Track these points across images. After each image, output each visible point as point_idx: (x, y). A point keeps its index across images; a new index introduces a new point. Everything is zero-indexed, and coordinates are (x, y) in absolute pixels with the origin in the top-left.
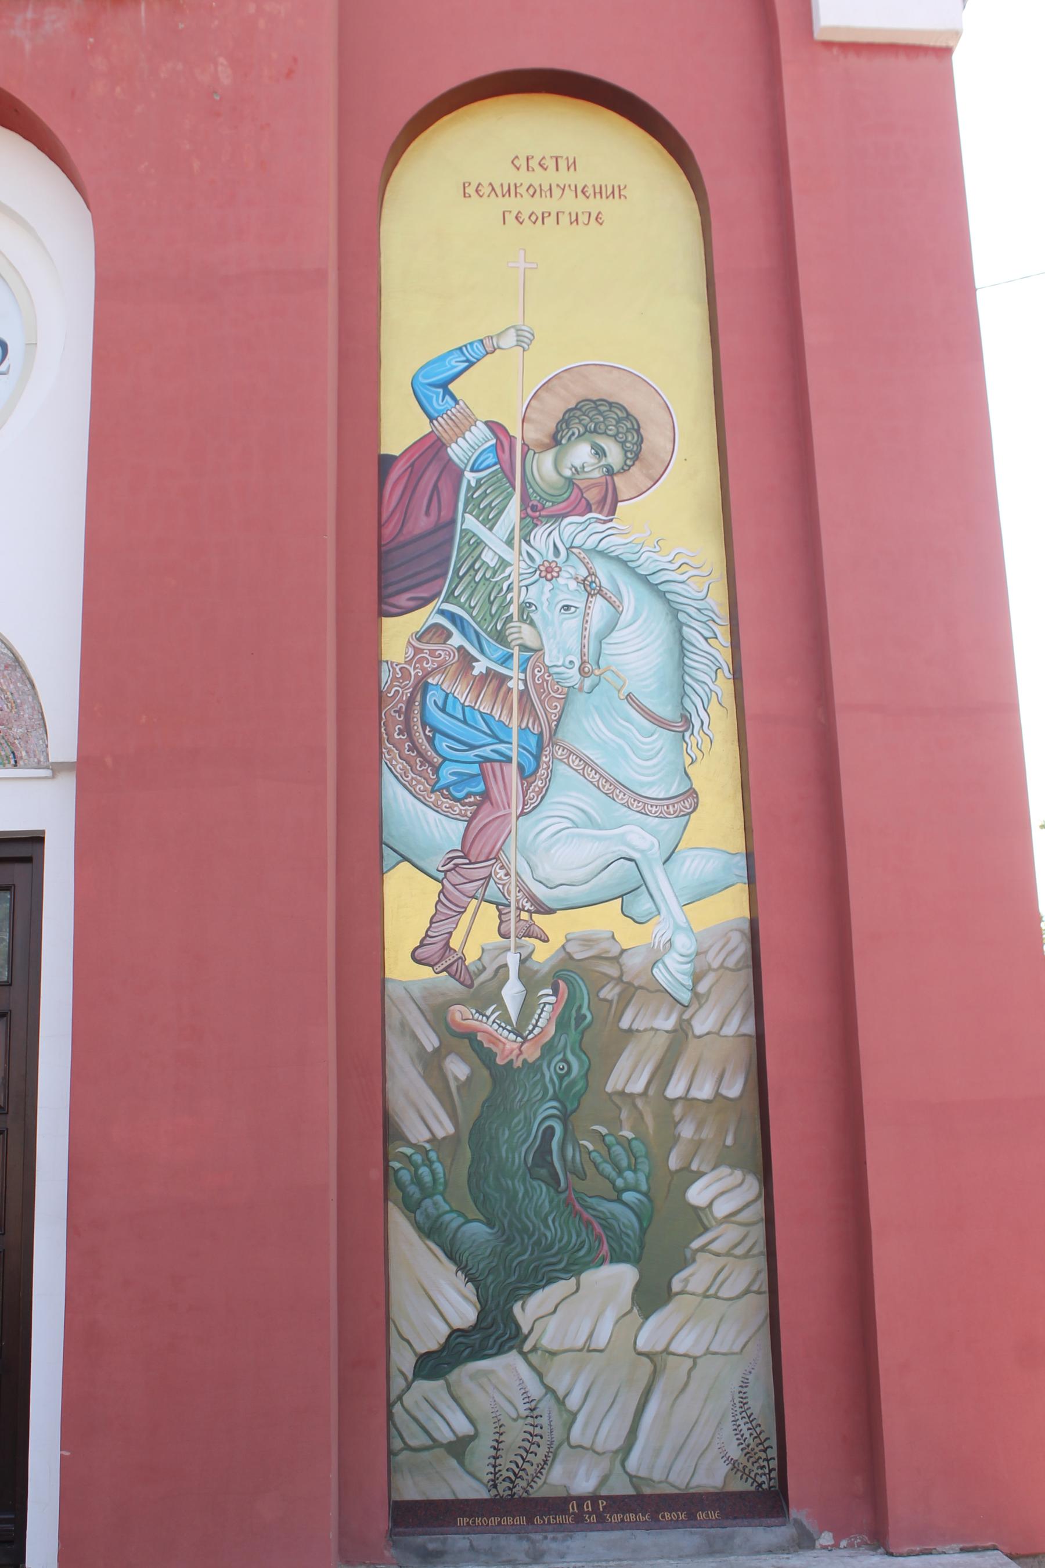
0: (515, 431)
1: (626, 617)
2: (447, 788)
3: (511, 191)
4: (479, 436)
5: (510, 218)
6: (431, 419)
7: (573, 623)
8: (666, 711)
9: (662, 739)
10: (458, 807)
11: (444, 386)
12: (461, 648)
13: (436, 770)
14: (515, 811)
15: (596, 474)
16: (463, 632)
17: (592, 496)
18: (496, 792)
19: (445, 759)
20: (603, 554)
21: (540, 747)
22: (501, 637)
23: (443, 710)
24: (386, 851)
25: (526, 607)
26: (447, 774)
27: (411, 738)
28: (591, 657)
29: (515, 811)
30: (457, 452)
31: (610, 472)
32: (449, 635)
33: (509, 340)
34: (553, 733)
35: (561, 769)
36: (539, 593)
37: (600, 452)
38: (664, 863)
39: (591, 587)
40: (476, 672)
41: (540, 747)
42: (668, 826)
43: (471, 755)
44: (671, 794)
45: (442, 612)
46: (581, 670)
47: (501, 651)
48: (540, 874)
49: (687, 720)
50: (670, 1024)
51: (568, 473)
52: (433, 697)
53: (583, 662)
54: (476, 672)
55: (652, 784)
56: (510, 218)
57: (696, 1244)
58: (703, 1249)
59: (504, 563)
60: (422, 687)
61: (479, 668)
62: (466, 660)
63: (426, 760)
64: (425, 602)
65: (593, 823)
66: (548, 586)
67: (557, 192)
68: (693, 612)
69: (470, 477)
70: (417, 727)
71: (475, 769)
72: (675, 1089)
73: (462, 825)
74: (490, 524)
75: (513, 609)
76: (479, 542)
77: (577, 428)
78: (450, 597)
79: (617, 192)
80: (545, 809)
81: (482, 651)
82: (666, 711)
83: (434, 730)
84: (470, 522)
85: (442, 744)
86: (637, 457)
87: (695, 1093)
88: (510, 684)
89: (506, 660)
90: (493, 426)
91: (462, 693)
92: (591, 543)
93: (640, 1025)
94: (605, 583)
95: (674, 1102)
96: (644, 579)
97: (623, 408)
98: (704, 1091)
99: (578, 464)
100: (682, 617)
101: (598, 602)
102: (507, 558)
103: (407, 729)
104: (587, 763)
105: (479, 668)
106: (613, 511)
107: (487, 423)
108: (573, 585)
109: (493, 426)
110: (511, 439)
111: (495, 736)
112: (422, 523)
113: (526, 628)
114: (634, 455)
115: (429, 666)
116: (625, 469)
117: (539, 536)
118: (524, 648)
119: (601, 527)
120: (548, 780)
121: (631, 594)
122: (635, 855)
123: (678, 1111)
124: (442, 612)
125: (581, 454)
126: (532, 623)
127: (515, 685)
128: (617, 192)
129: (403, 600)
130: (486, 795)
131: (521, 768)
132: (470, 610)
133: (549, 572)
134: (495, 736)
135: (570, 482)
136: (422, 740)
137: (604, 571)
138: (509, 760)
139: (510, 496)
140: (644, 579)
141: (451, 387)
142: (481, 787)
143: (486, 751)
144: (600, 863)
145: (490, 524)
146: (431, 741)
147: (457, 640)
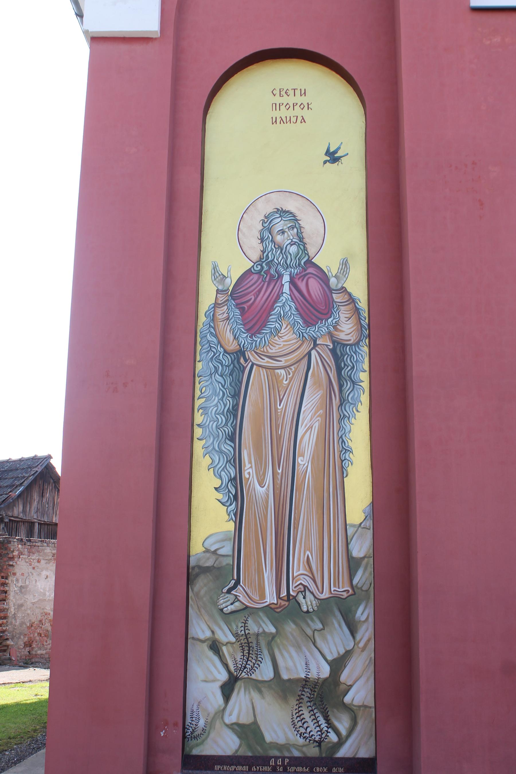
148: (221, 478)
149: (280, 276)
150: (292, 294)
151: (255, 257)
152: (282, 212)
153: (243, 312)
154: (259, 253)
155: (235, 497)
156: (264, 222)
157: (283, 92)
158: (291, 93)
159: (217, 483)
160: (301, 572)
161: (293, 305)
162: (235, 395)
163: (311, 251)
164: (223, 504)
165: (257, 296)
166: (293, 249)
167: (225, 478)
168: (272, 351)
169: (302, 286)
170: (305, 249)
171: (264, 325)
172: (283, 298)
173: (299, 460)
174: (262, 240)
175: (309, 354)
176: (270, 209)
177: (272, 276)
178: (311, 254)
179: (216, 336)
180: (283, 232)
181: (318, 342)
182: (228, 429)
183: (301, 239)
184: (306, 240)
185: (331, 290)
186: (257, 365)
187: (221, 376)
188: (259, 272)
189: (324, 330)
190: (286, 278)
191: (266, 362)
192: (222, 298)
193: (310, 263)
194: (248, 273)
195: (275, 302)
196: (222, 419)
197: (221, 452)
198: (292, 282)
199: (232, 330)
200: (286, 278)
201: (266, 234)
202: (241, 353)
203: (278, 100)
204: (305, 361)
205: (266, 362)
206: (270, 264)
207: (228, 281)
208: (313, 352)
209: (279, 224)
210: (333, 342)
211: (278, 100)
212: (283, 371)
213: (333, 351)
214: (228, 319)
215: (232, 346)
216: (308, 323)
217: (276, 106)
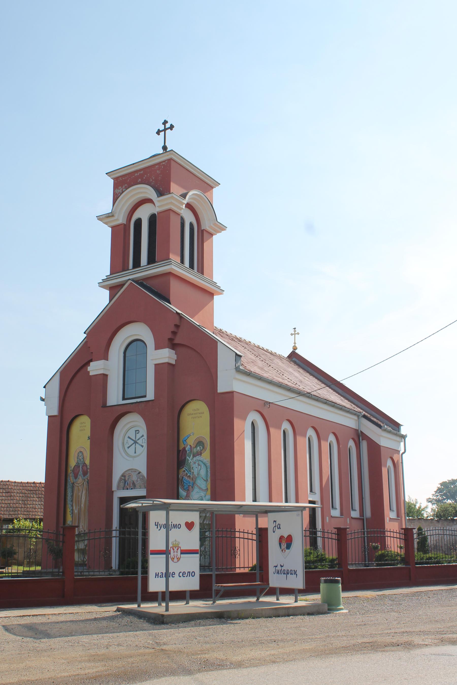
0: (192, 446)
1: (202, 468)
2: (185, 489)
3: (192, 414)
4: (189, 446)
5: (192, 418)
6: (184, 445)
7: (197, 469)
8: (205, 479)
9: (205, 482)
10: (186, 491)
11: (185, 440)
12: (186, 473)
13: (184, 487)
14: (191, 492)
15: (200, 451)
16: (187, 471)
17: (199, 453)
18: (189, 490)
19: (185, 486)
20: (200, 460)
21: (194, 484)
22: (190, 471)
23: (185, 480)
24: (179, 496)
25: (192, 467)
26: (185, 488)
27: (182, 483)
28: (198, 473)
29: (191, 492)
30: (187, 449)
31: (201, 450)
32: (185, 471)
33: (192, 434)
34: (195, 482)
35: (195, 486)
36: (194, 466)
37: (200, 448)
38: (205, 497)
39: (199, 465)
40: (188, 475)
41: (194, 484)
42: (205, 493)
43: (187, 485)
44: (206, 489)
45: (185, 469)
46: (198, 475)
47: (190, 473)
48: (193, 498)
49: (207, 480)
50: (204, 515)
51: (197, 451)
52: (184, 479)
53: (198, 474)
54: (188, 475)
55: (203, 488)
56: (192, 418)
57: (206, 539)
58: (207, 540)
59: (191, 462)
60: (183, 478)
61: (188, 475)
62: (187, 474)
63: (183, 486)
64: (183, 467)
65: (198, 493)
66: (195, 465)
67: (197, 414)
68: (208, 467)
69: (188, 452)
70: (182, 482)
71: (187, 487)
72: (205, 523)
73: (186, 493)
74: (190, 458)
75: (191, 468)
76: (188, 460)
77: (198, 445)
78: (186, 467)
79: (203, 413)
80: (194, 491)
81: (188, 473)
82: (205, 479)
83: (184, 482)
84: (188, 458)
85: (185, 484)
86: (204, 447)
87: (207, 523)
88: (191, 477)
89: (190, 474)
90: (190, 445)
91: (186, 478)
92: (199, 459)
93: (202, 515)
94: (200, 464)
95: (205, 524)
96: (204, 463)
97: (202, 442)
98: (207, 523)
99: (198, 449)
100: (207, 468)
101: (199, 466)
102: (191, 462)
103: (181, 482)
104: (198, 486)
105: (188, 475)
106: (201, 455)
107: (190, 445)
108: (197, 464)
109: (190, 445)
110: (192, 447)
111: (189, 483)
112: (183, 458)
113: (192, 470)
114: (203, 448)
115: (183, 475)
116: (203, 450)
117: (194, 458)
118: (192, 472)
119: (200, 457)
120: (194, 488)
121: (203, 465)
122: (202, 496)
123: (205, 525)
124: (185, 469)
125: (198, 448)
126: (193, 469)
127: (191, 477)
128: (203, 413)
129: (181, 467)
130: (188, 490)
131: (192, 486)
132: (187, 468)
133: (195, 463)
134: (189, 483)
135: (197, 452)
136: (183, 484)
137: (200, 462)
138: (190, 486)
139: (191, 455)
140: (204, 463)
141: (186, 441)
142: (188, 489)
143: (189, 485)
144: (198, 497)
145: (190, 458)
146: (184, 484)
147: (186, 472)
148: (70, 509)
149: (80, 466)
150: (82, 470)
151: (76, 462)
152: (81, 452)
153: (74, 474)
154: (77, 461)
155: (72, 513)
156: (78, 454)
157: (82, 423)
158: (83, 423)
159: (69, 510)
160: (82, 528)
161: (82, 472)
162: (72, 492)
163: (85, 460)
164: (70, 515)
165: (76, 471)
166: (82, 460)
167: (71, 510)
168: (78, 482)
169: (83, 468)
170: (84, 460)
171: (77, 477)
172: (80, 471)
173: (82, 505)
174: (77, 458)
175: (84, 483)
176: (79, 451)
177: (79, 466)
178: (85, 461)
179: (70, 480)
180: (81, 456)
181: (85, 480)
182: (71, 499)
183: (83, 458)
184: (84, 458)
185: (88, 468)
186: (76, 486)
187: (71, 488)
188: (77, 466)
189: (86, 477)
190: (81, 467)
191: (77, 485)
192: (71, 471)
193: (85, 463)
194: (75, 466)
195: (79, 472)
196: (70, 497)
197: (70, 504)
198: (82, 468)
199: (72, 478)
200: (81, 467)
201: (78, 457)
202: (73, 483)
203: (81, 425)
204: (83, 484)
205: (77, 485)
206: (78, 463)
207: (72, 468)
208: (85, 482)
209: (80, 454)
210: (88, 480)
211: (81, 425)
212: (80, 487)
213: (87, 482)
214: (72, 476)
215: (72, 482)
216: (84, 476)
217: (80, 427)
